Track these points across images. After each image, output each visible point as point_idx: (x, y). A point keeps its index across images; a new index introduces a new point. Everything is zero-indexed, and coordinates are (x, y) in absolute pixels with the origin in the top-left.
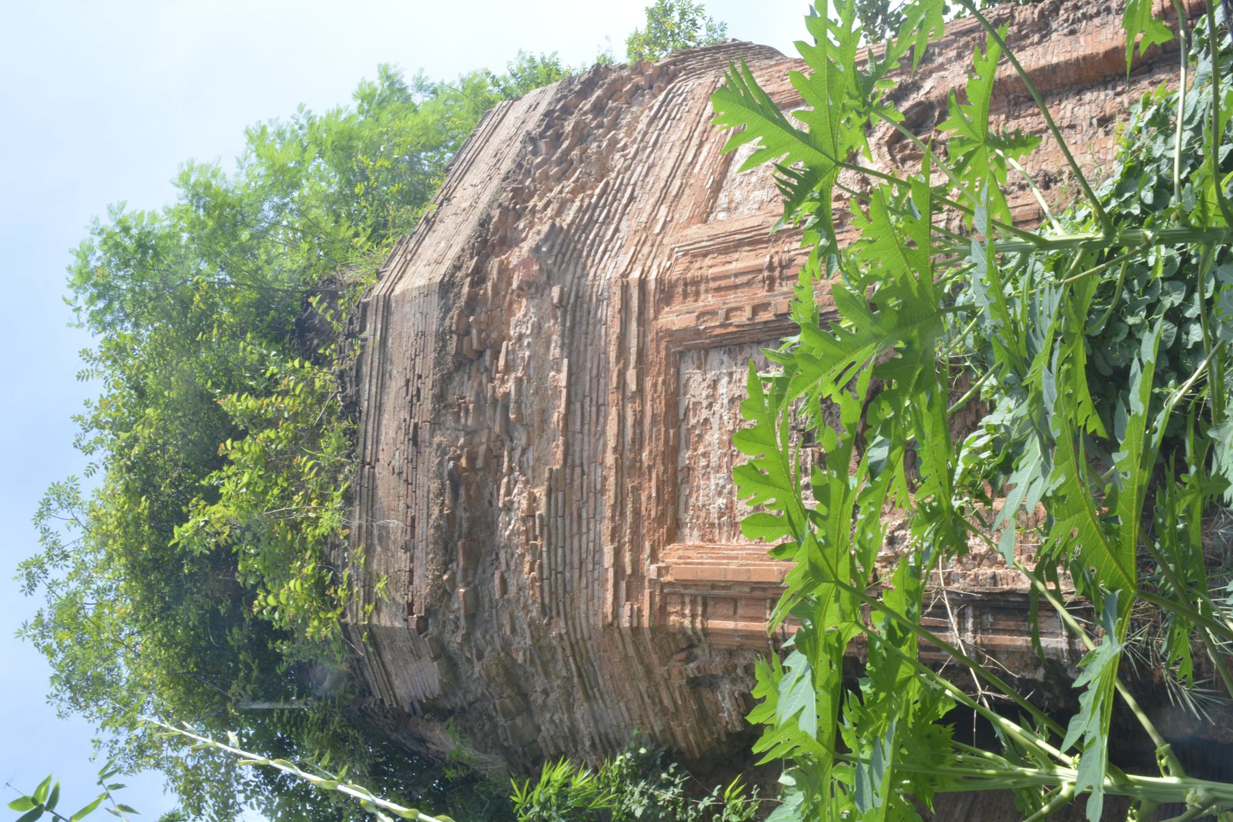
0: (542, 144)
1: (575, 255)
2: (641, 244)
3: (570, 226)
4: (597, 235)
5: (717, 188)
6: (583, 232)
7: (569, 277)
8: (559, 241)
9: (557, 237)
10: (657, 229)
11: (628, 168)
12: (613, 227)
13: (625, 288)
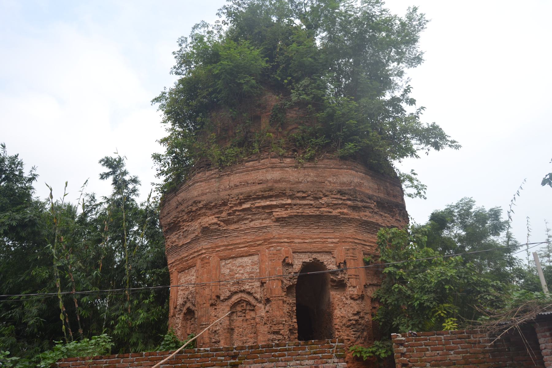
0: (238, 201)
2: (212, 248)
5: (233, 258)
7: (200, 235)
10: (217, 250)
13: (201, 250)
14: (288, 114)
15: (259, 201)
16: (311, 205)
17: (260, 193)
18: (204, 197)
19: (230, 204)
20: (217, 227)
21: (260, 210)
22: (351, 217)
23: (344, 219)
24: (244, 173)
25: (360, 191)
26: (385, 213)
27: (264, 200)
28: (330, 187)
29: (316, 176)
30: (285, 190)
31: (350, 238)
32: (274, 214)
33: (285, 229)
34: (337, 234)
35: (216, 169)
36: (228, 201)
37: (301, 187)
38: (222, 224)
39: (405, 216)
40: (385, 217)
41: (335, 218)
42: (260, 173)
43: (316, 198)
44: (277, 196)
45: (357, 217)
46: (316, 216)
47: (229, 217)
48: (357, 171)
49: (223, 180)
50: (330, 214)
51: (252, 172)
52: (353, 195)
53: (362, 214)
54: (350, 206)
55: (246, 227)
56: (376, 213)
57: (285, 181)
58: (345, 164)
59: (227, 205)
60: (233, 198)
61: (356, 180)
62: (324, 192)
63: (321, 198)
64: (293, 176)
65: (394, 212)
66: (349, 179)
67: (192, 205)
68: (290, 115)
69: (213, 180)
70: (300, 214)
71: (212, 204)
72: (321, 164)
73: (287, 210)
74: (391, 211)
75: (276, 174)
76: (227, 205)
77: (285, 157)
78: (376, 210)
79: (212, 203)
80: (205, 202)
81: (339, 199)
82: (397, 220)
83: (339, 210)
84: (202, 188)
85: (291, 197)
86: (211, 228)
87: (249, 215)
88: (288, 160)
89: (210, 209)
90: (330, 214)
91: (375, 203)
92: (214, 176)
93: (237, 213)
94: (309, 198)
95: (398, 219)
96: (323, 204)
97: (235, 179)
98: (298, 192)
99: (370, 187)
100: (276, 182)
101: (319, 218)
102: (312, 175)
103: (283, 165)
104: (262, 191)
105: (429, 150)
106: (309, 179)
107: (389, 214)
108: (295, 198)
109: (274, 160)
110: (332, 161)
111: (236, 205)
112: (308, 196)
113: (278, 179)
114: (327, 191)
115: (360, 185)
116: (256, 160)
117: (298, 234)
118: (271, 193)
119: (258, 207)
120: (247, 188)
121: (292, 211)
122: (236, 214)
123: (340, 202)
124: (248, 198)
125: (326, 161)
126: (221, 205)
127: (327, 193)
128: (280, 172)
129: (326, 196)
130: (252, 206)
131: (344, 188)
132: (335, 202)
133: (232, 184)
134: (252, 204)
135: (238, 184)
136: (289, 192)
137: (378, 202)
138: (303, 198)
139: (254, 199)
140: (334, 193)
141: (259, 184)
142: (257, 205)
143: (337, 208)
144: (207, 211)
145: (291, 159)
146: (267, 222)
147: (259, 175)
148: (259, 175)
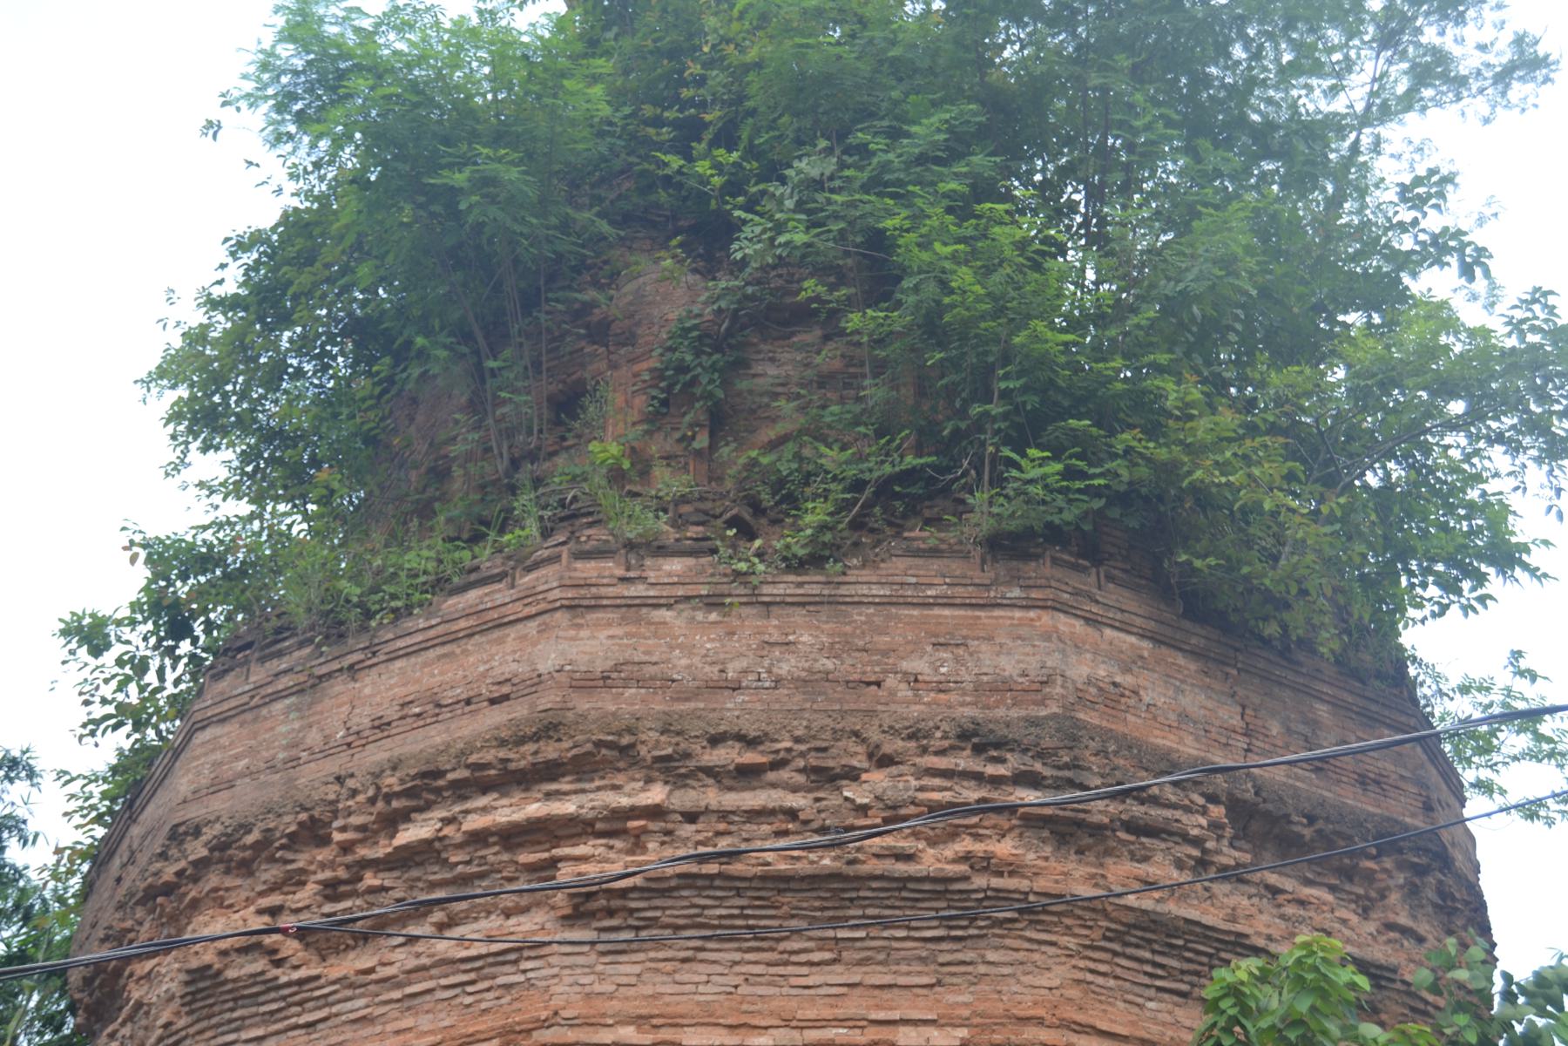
1: (205, 1011)
3: (226, 981)
4: (243, 1018)
6: (235, 1000)
7: (182, 1023)
8: (201, 985)
9: (203, 978)
11: (352, 986)
12: (260, 1032)
14: (758, 369)
15: (482, 801)
16: (792, 814)
17: (489, 756)
18: (219, 804)
19: (343, 829)
20: (259, 964)
21: (492, 854)
22: (1041, 884)
23: (1001, 896)
24: (432, 654)
25: (1107, 735)
26: (1308, 883)
27: (517, 796)
28: (916, 710)
29: (831, 651)
30: (630, 730)
31: (1040, 1021)
32: (565, 873)
33: (627, 968)
34: (959, 998)
35: (301, 645)
36: (335, 814)
37: (734, 710)
38: (291, 947)
39: (1465, 911)
40: (1302, 903)
41: (938, 895)
42: (510, 644)
43: (825, 777)
44: (583, 767)
45: (1085, 891)
46: (815, 880)
47: (327, 908)
48: (1090, 621)
49: (327, 703)
50: (902, 868)
51: (469, 645)
52: (1054, 752)
53: (1120, 871)
54: (1032, 822)
55: (412, 963)
56: (1234, 875)
57: (640, 682)
58: (1014, 579)
59: (325, 841)
60: (354, 793)
61: (1080, 669)
62: (874, 736)
63: (853, 775)
64: (689, 650)
65: (1369, 877)
66: (1032, 664)
67: (163, 856)
68: (772, 371)
69: (278, 706)
70: (712, 868)
71: (250, 839)
72: (863, 582)
73: (644, 850)
74: (1349, 874)
75: (592, 644)
76: (325, 841)
77: (662, 551)
78: (1229, 856)
79: (247, 828)
80: (218, 828)
81: (966, 775)
82: (1390, 926)
83: (965, 844)
84: (218, 756)
85: (670, 768)
86: (231, 974)
87: (433, 886)
88: (675, 566)
89: (246, 868)
90: (902, 868)
91: (1218, 811)
92: (285, 682)
93: (370, 880)
94: (784, 774)
95: (1403, 920)
96: (863, 810)
97: (381, 689)
98: (715, 741)
99: (1184, 716)
100: (588, 683)
101: (837, 889)
102: (808, 642)
103: (638, 590)
104: (503, 743)
105: (1559, 491)
106: (787, 666)
107: (1332, 889)
108: (691, 774)
109: (588, 569)
110: (936, 565)
111: (367, 833)
112: (776, 765)
113: (600, 666)
114: (892, 731)
115: (1113, 697)
116: (500, 577)
117: (708, 994)
118: (550, 751)
119: (478, 838)
120: (432, 731)
121: (668, 852)
122: (362, 886)
123: (971, 794)
124: (427, 787)
125: (900, 564)
126: (293, 841)
127: (892, 746)
128: (619, 631)
129: (885, 761)
130: (448, 831)
131: (1000, 712)
132: (936, 796)
133: (362, 719)
134: (447, 821)
135: (392, 713)
136: (653, 743)
137: (1236, 807)
138: (747, 775)
139: (462, 790)
140: (937, 743)
141: (493, 702)
142: (474, 823)
143: (953, 835)
144: (229, 882)
145: (691, 561)
146: (524, 926)
147: (500, 658)
148: (500, 658)
